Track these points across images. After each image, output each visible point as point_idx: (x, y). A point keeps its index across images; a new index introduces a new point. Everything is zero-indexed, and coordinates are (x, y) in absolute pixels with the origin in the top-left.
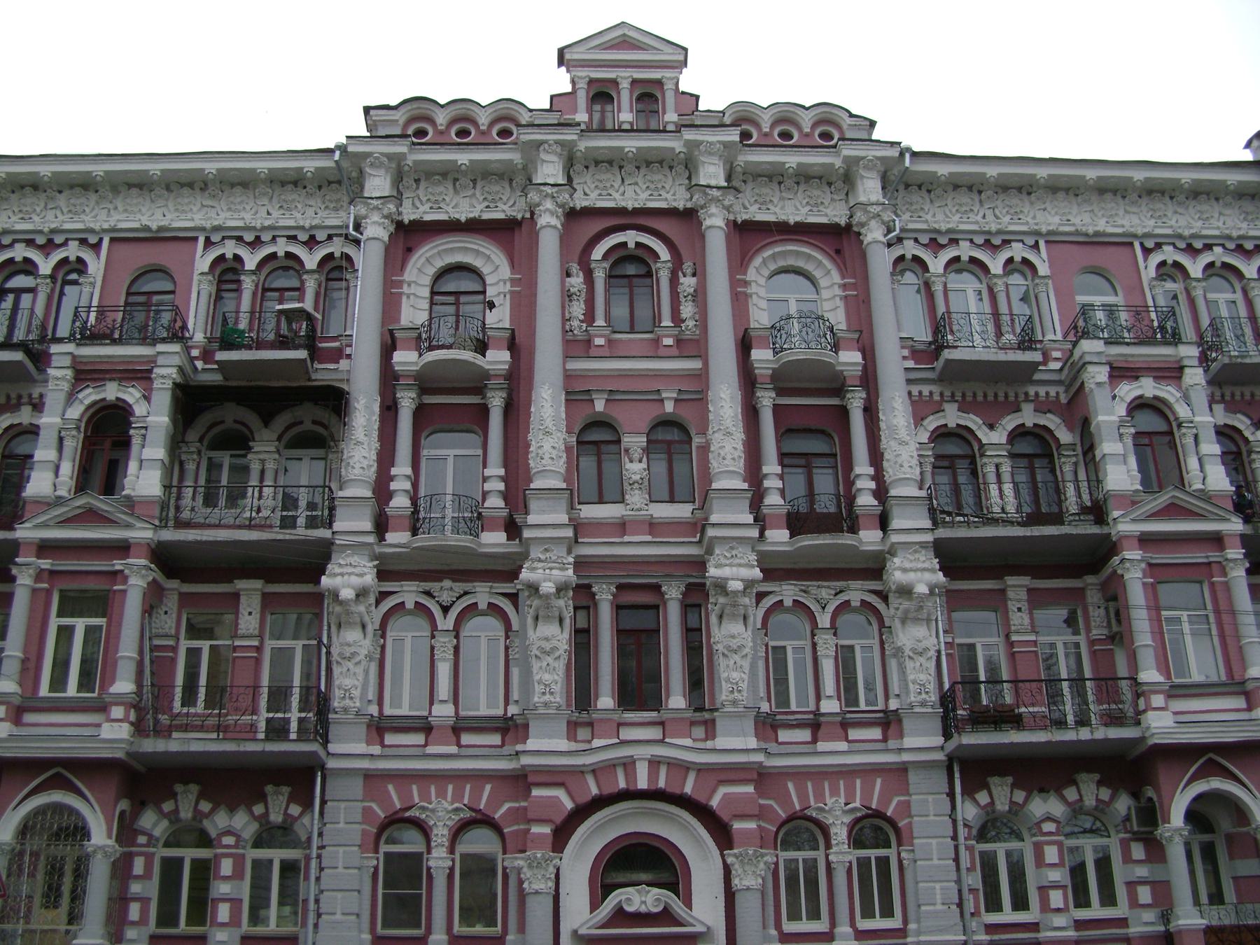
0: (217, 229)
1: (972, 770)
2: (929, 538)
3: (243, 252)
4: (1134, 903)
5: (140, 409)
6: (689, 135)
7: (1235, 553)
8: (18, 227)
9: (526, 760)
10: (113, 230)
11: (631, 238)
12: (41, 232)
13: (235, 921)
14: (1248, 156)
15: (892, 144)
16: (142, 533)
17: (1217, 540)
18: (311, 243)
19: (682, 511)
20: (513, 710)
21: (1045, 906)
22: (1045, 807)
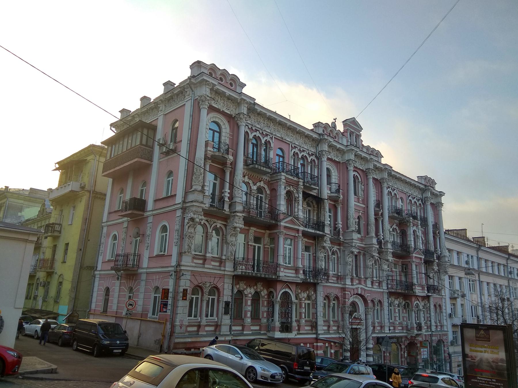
0: (294, 143)
1: (390, 294)
2: (392, 251)
3: (298, 152)
4: (403, 320)
5: (297, 195)
6: (372, 157)
7: (423, 261)
8: (257, 126)
9: (347, 286)
10: (275, 135)
11: (356, 174)
12: (262, 130)
13: (305, 317)
14: (416, 180)
15: (391, 167)
16: (301, 228)
17: (421, 259)
18: (310, 155)
19: (359, 236)
20: (340, 274)
21: (395, 320)
22: (397, 302)
